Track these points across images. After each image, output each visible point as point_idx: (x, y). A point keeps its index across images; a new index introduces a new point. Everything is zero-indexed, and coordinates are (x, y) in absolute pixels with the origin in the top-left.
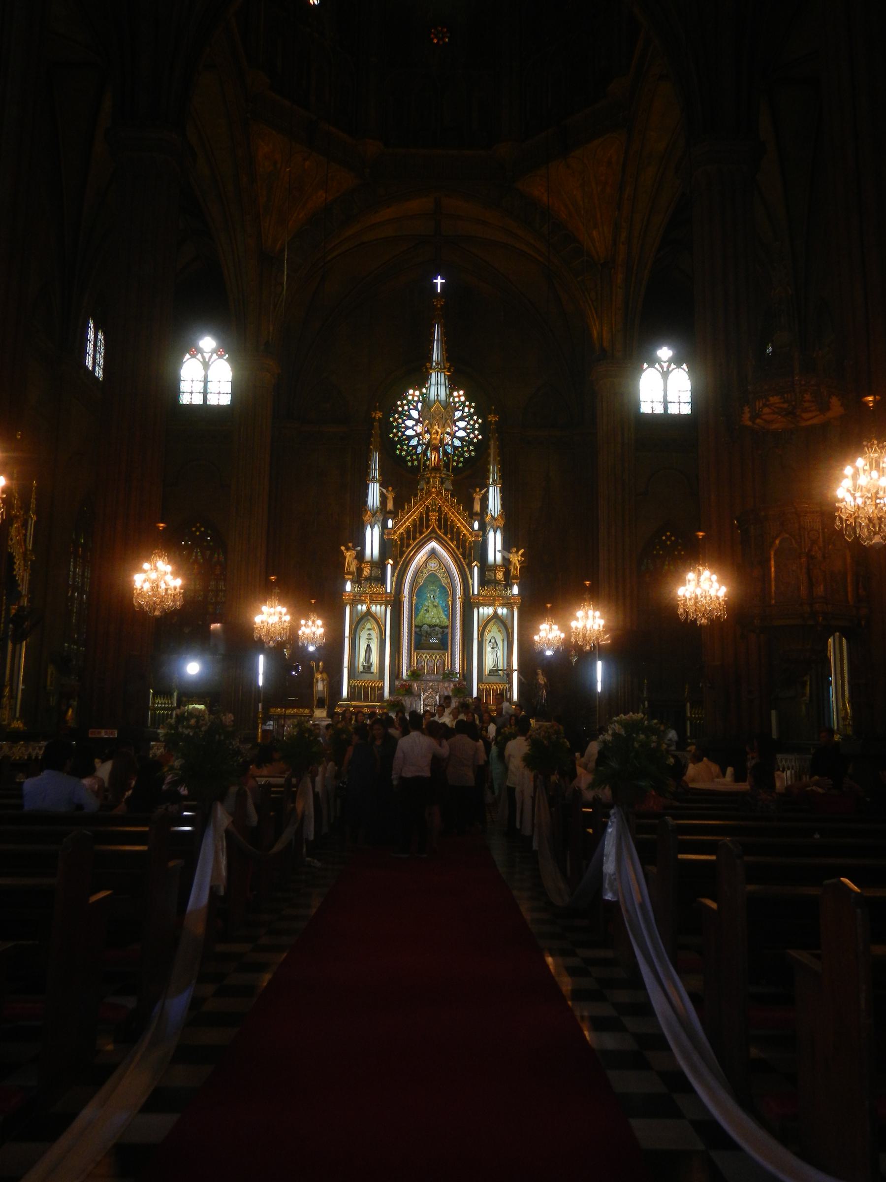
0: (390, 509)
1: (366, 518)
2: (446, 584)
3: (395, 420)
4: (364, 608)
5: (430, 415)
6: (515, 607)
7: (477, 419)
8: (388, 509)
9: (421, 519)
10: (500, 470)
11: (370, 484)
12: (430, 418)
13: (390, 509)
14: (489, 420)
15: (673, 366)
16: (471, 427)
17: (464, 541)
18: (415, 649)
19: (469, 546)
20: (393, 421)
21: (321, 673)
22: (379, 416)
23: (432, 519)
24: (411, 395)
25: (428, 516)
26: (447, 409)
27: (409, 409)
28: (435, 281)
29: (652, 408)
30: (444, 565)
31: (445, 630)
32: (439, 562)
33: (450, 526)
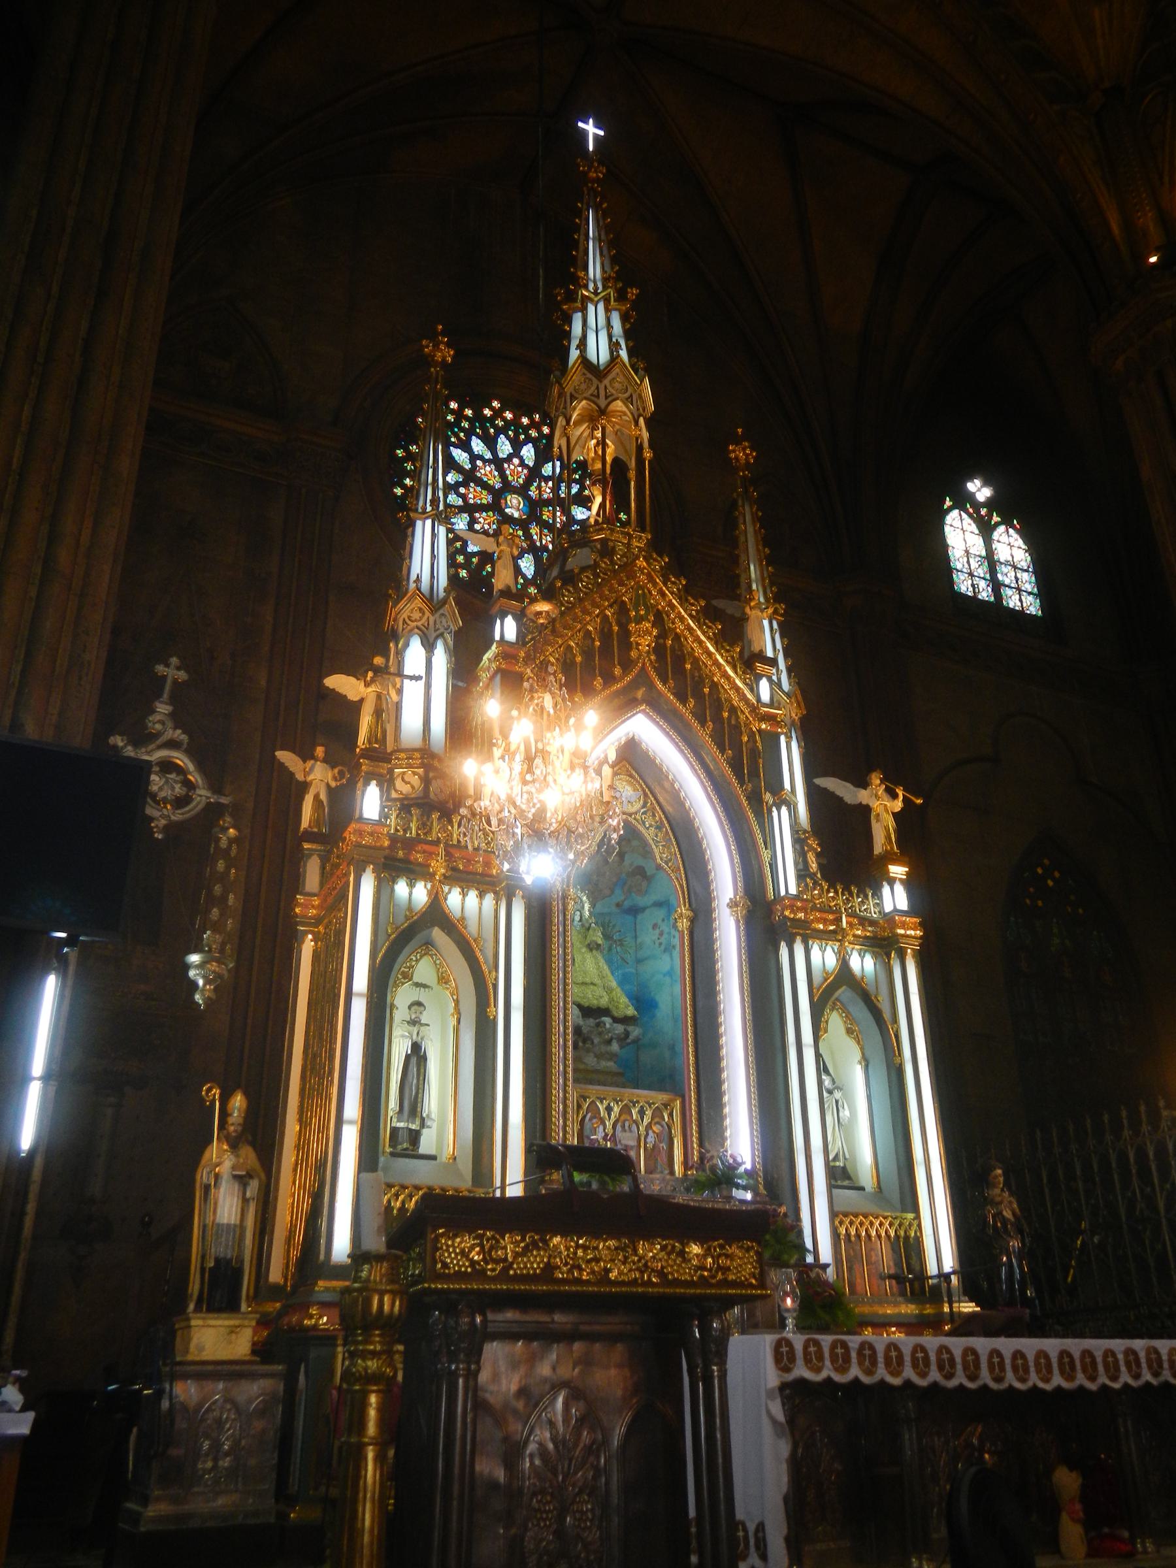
1: (405, 616)
2: (666, 863)
4: (420, 894)
5: (598, 388)
6: (909, 951)
9: (606, 635)
11: (419, 524)
12: (598, 397)
15: (996, 518)
17: (736, 729)
18: (576, 1081)
19: (750, 745)
21: (234, 1146)
22: (444, 358)
25: (625, 633)
29: (973, 585)
30: (656, 799)
31: (630, 1028)
32: (644, 791)
33: (693, 677)
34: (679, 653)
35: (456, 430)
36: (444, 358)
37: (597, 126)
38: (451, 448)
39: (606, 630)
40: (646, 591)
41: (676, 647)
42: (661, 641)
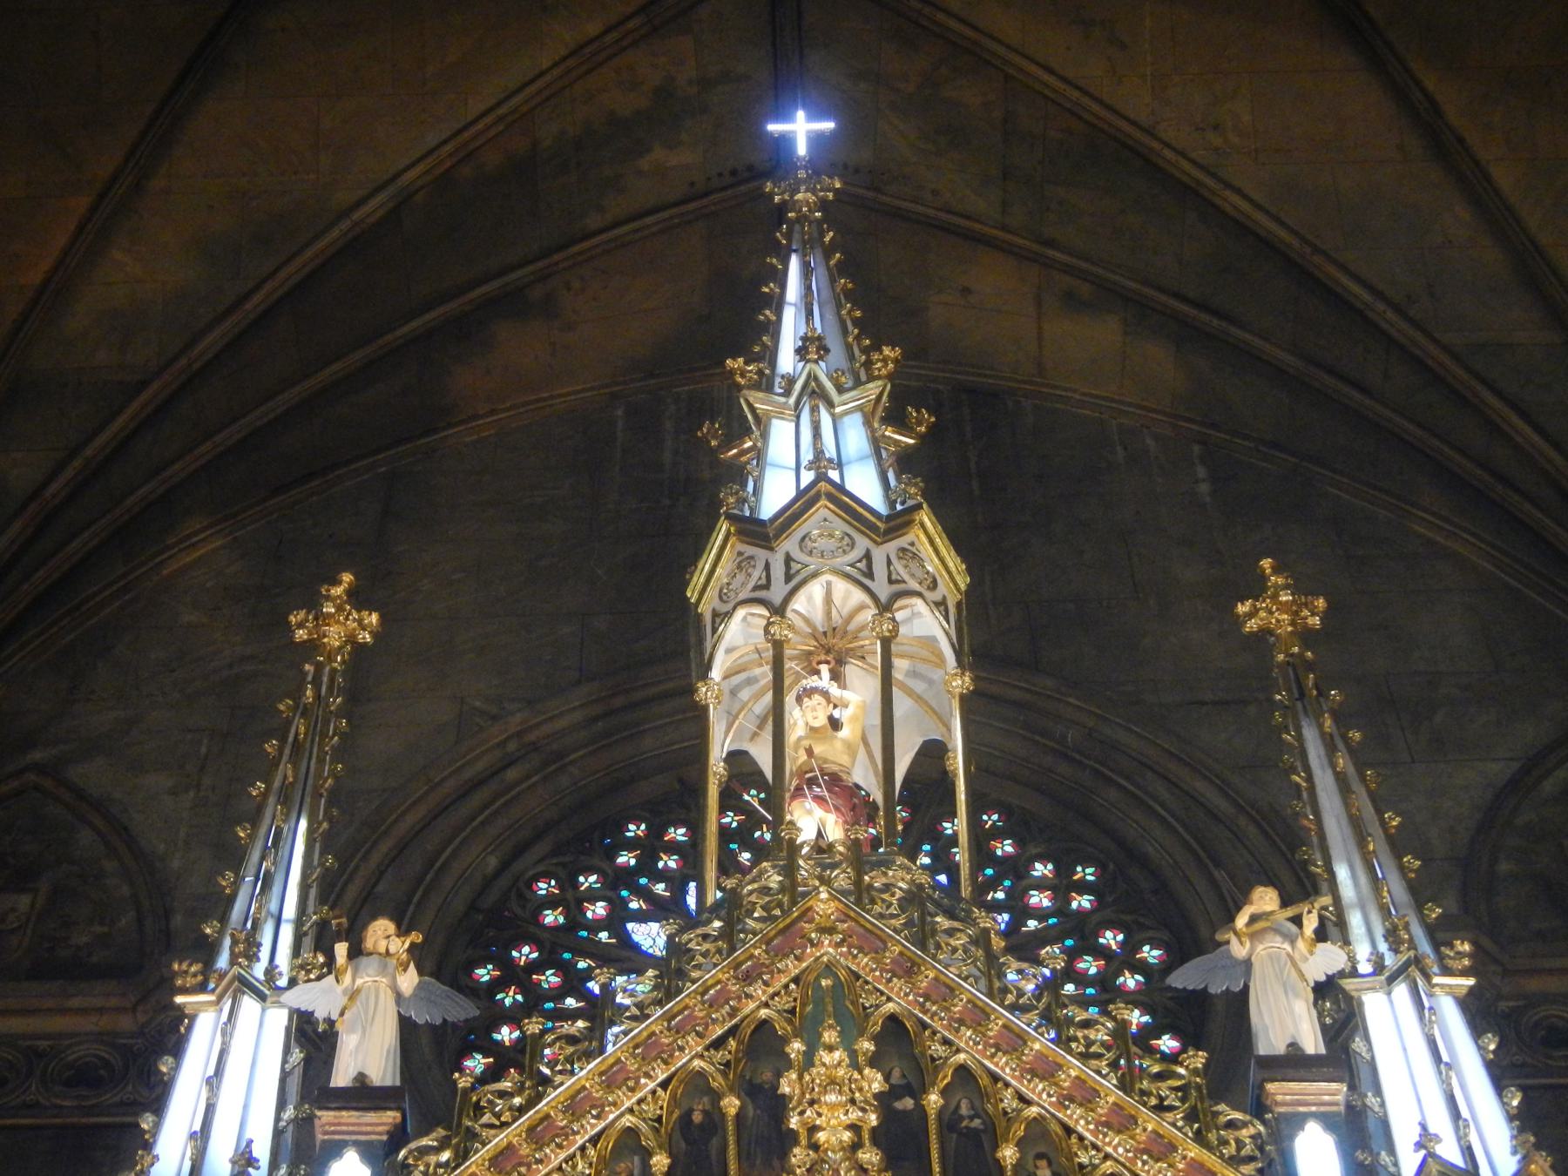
0: (361, 1077)
3: (511, 975)
5: (767, 567)
7: (1130, 946)
8: (342, 1077)
10: (1419, 893)
12: (767, 586)
13: (361, 1077)
14: (1252, 625)
16: (1090, 991)
20: (498, 985)
23: (813, 1129)
24: (630, 845)
26: (902, 542)
27: (617, 919)
28: (773, 127)
34: (977, 1123)
35: (643, 881)
36: (351, 639)
37: (813, 116)
38: (630, 926)
39: (697, 1117)
40: (842, 974)
41: (964, 1111)
42: (908, 1103)
